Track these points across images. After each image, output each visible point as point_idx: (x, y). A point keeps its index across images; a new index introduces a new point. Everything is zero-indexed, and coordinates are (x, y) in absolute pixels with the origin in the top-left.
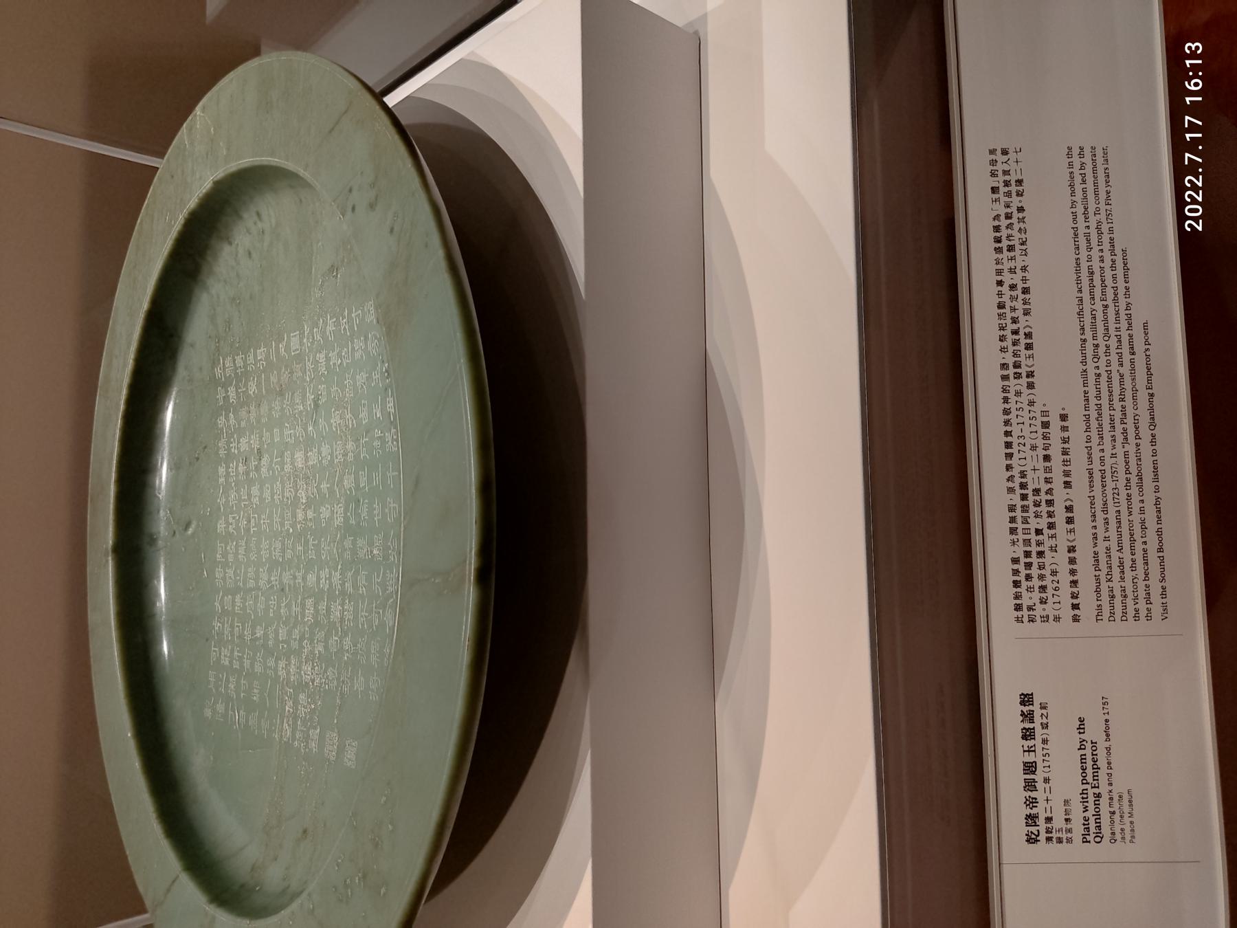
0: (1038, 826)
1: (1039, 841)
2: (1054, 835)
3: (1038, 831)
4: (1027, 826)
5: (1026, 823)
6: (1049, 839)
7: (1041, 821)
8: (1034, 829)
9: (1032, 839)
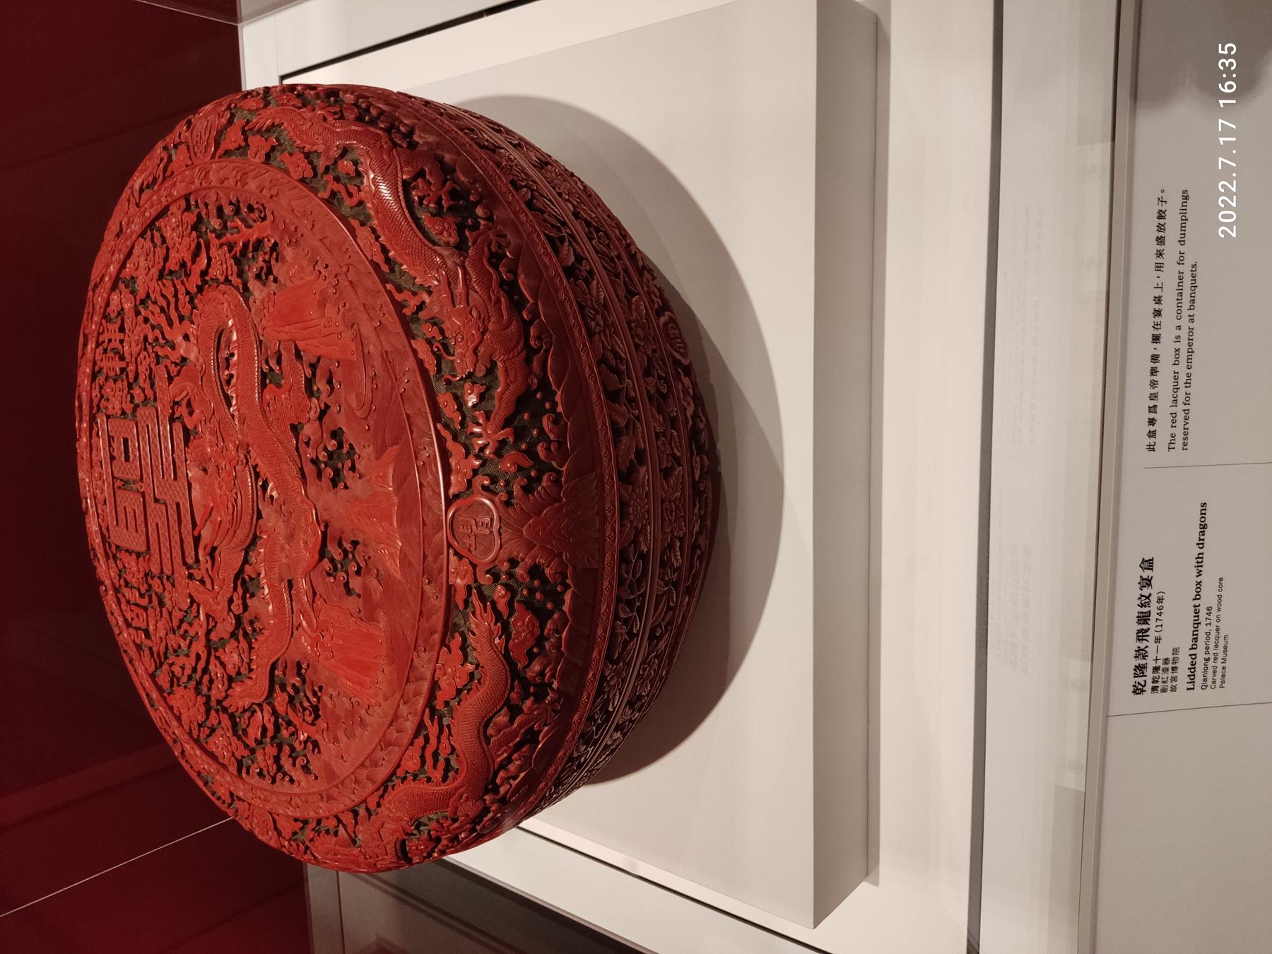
0: (1146, 676)
1: (1145, 691)
4: (1135, 677)
7: (1149, 672)
8: (1141, 680)
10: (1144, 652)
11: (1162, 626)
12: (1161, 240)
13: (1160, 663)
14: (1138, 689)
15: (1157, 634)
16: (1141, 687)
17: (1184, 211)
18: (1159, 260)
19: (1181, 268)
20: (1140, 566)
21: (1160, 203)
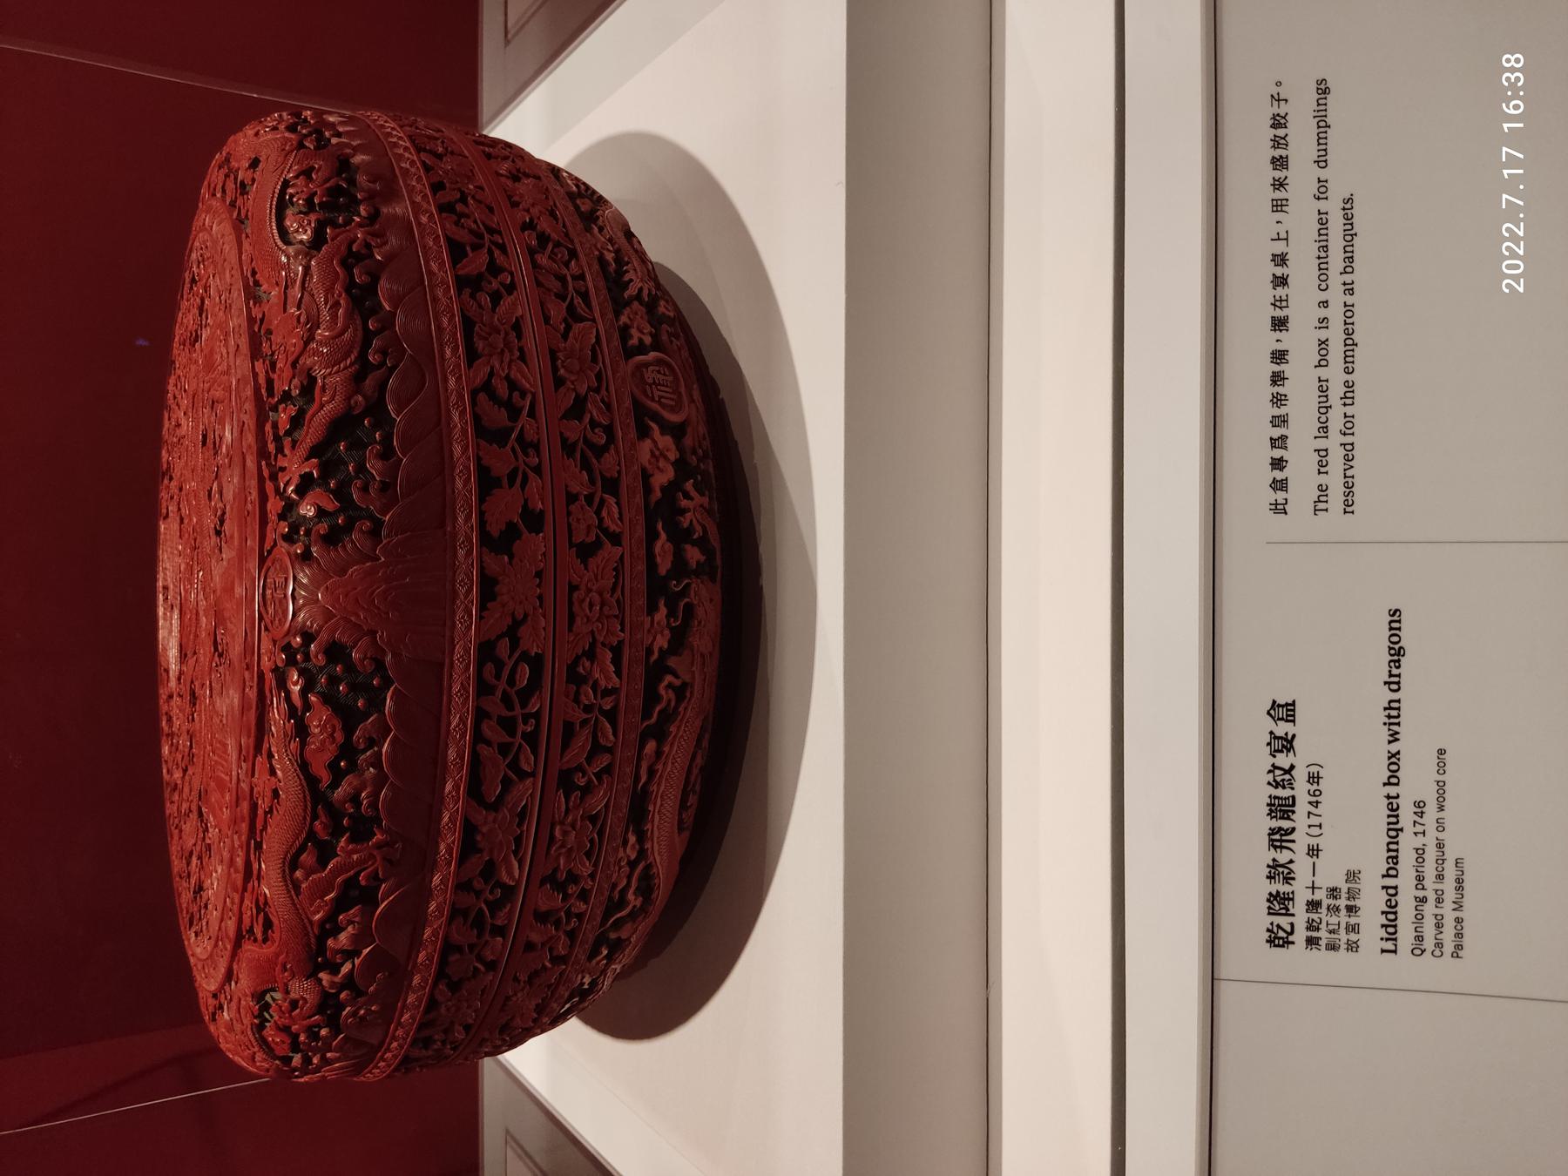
0: (1293, 915)
1: (1293, 943)
4: (1269, 914)
5: (1269, 908)
6: (1312, 942)
7: (1299, 908)
8: (1284, 921)
9: (1278, 939)
10: (1286, 871)
11: (1320, 826)
12: (1280, 163)
13: (1320, 895)
14: (1279, 938)
15: (1313, 841)
16: (1285, 935)
17: (1323, 113)
18: (1279, 195)
19: (1323, 205)
20: (1269, 713)
21: (1275, 103)
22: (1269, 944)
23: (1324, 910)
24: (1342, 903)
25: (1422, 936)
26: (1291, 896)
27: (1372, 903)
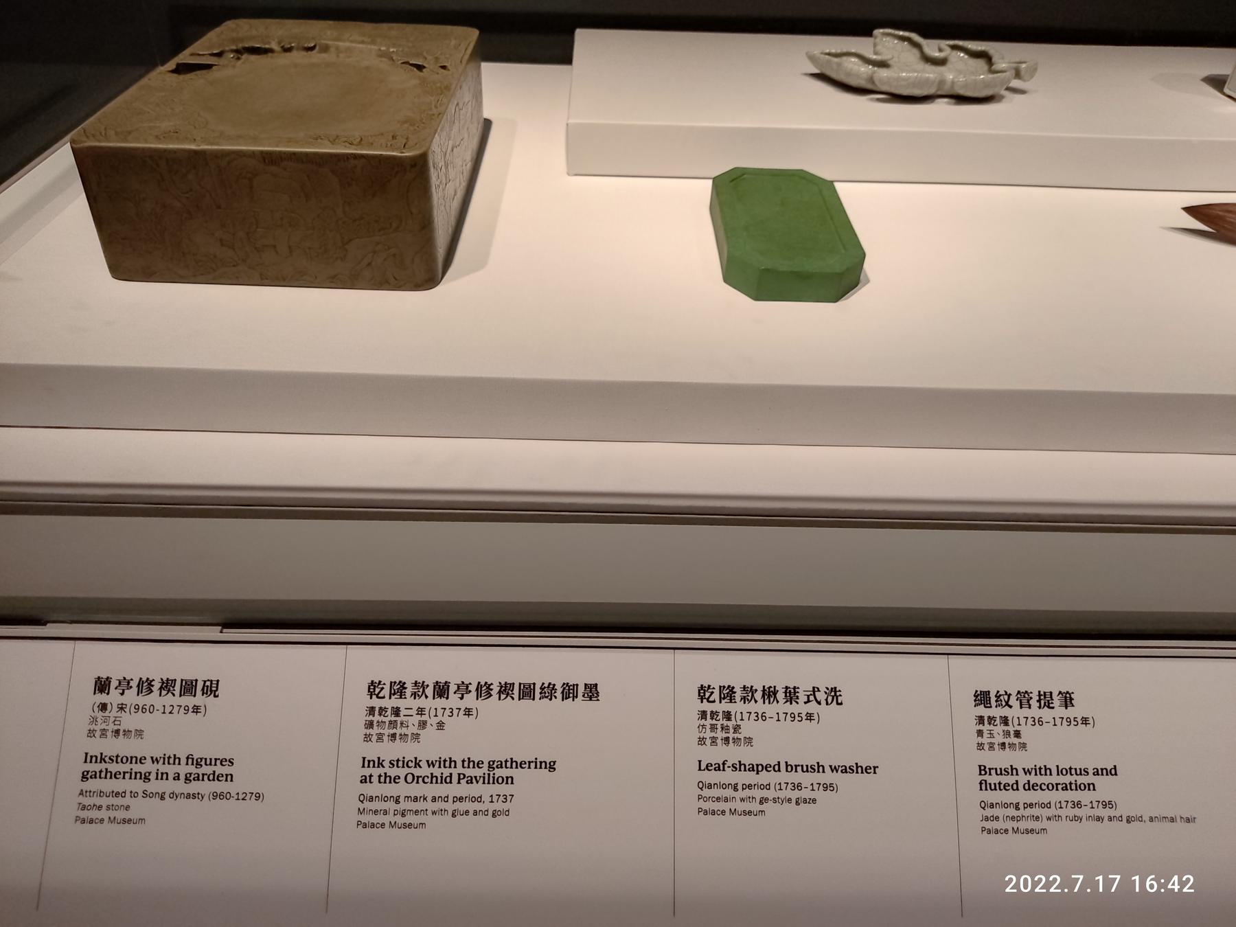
1: (702, 702)
2: (709, 722)
3: (714, 701)
4: (720, 687)
5: (724, 687)
6: (703, 715)
8: (716, 696)
16: (707, 697)
22: (700, 686)
23: (725, 723)
24: (731, 735)
25: (711, 788)
26: (733, 701)
27: (733, 754)
